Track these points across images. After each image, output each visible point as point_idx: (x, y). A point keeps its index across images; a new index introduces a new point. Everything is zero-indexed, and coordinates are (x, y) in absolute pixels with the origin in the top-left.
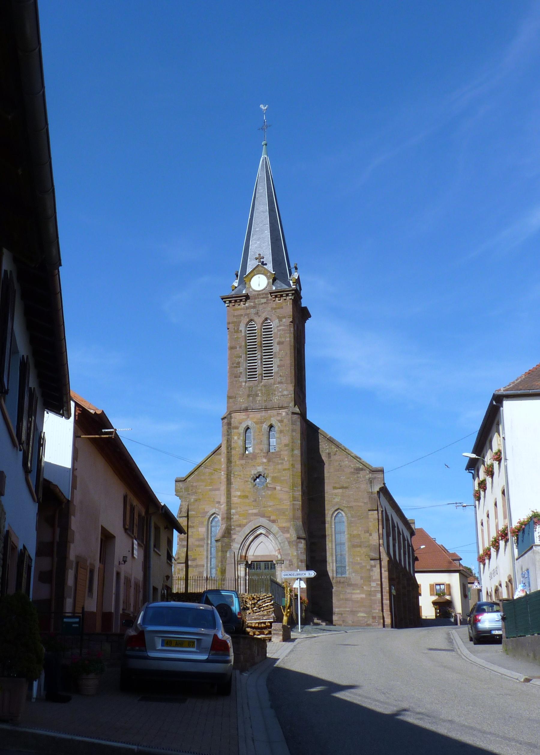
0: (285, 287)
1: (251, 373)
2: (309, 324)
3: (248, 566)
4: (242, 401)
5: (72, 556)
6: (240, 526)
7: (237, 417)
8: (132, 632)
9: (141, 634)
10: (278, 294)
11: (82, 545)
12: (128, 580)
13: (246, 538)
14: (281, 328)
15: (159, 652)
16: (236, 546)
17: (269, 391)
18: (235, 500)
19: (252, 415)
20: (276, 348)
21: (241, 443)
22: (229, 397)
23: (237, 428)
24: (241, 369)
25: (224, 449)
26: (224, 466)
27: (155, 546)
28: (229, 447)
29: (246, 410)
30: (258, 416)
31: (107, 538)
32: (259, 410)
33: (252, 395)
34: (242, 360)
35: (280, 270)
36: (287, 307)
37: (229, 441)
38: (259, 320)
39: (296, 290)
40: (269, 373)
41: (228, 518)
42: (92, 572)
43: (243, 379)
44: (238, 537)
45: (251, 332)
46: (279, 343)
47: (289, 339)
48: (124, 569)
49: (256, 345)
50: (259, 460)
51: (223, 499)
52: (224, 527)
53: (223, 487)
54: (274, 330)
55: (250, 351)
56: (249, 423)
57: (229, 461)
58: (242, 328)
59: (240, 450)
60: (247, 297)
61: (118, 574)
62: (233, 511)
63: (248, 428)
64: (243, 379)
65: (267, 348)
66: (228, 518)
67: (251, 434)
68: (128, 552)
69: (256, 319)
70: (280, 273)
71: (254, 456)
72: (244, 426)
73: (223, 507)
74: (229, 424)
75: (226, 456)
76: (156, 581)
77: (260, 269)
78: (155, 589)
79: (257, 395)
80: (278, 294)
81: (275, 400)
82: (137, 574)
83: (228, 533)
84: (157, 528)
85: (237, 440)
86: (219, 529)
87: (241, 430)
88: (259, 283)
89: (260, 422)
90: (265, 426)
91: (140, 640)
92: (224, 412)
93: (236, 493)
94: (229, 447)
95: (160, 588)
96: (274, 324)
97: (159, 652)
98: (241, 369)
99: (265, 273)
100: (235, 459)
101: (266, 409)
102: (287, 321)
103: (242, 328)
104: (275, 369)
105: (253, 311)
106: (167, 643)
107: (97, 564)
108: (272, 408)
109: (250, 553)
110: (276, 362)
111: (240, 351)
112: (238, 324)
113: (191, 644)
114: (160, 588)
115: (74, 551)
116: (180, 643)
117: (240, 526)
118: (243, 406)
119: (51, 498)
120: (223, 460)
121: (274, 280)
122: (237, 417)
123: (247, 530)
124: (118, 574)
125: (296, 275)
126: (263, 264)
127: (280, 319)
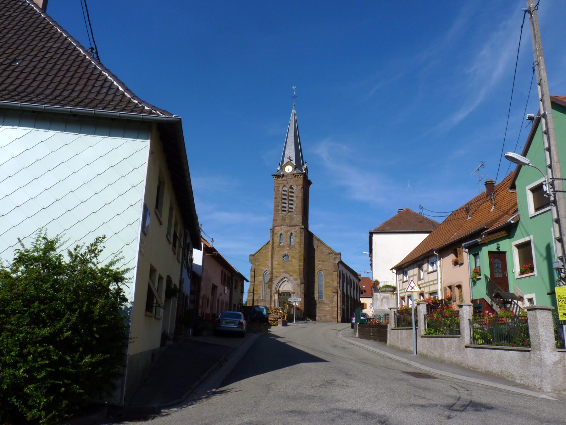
0: (300, 172)
1: (284, 210)
2: (311, 187)
3: (279, 294)
4: (279, 222)
5: (201, 294)
6: (276, 277)
7: (277, 229)
8: (217, 319)
9: (219, 320)
10: (297, 175)
11: (205, 291)
12: (222, 302)
13: (279, 282)
14: (297, 190)
15: (224, 325)
16: (274, 286)
17: (291, 218)
18: (275, 266)
19: (283, 228)
20: (295, 199)
21: (278, 240)
22: (274, 220)
23: (276, 234)
24: (280, 208)
25: (271, 243)
26: (270, 250)
27: (235, 288)
28: (273, 242)
29: (281, 226)
30: (286, 229)
31: (214, 287)
32: (287, 226)
33: (284, 219)
34: (280, 204)
35: (299, 161)
36: (300, 180)
37: (273, 239)
38: (288, 186)
39: (305, 173)
40: (291, 210)
41: (272, 273)
42: (208, 300)
43: (280, 212)
44: (275, 282)
45: (284, 192)
46: (296, 197)
47: (300, 195)
48: (221, 298)
49: (286, 197)
50: (285, 249)
51: (270, 265)
52: (269, 277)
53: (270, 260)
54: (295, 191)
55: (283, 200)
56: (282, 232)
57: (273, 248)
58: (280, 189)
59: (278, 244)
60: (283, 175)
61: (218, 300)
62: (274, 271)
63: (281, 234)
64: (280, 212)
65: (290, 198)
66: (272, 273)
67: (283, 236)
68: (224, 292)
69: (287, 185)
70: (298, 166)
71: (283, 247)
72: (279, 233)
73: (269, 269)
74: (273, 232)
75: (272, 245)
76: (235, 301)
77: (288, 163)
78: (235, 305)
79: (286, 220)
80: (297, 175)
81: (294, 222)
82: (227, 299)
83: (271, 280)
84: (236, 281)
85: (277, 240)
86: (268, 278)
87: (278, 235)
88: (289, 169)
89: (287, 232)
90: (289, 234)
91: (219, 322)
92: (271, 227)
93: (275, 263)
94: (273, 242)
95: (237, 304)
96: (295, 188)
97: (224, 325)
98: (280, 208)
99: (292, 165)
100: (275, 247)
101: (290, 226)
102: (300, 187)
103: (280, 189)
104: (294, 208)
105: (285, 182)
106: (226, 322)
107: (210, 296)
108: (292, 226)
109: (281, 289)
110: (295, 205)
111: (279, 200)
112: (278, 187)
113: (233, 323)
114: (237, 304)
115: (202, 293)
116: (230, 323)
117: (276, 277)
118: (280, 224)
119: (195, 276)
120: (270, 248)
121: (295, 168)
122: (277, 229)
123: (280, 279)
124: (218, 300)
125: (305, 166)
126: (291, 160)
127: (297, 186)
